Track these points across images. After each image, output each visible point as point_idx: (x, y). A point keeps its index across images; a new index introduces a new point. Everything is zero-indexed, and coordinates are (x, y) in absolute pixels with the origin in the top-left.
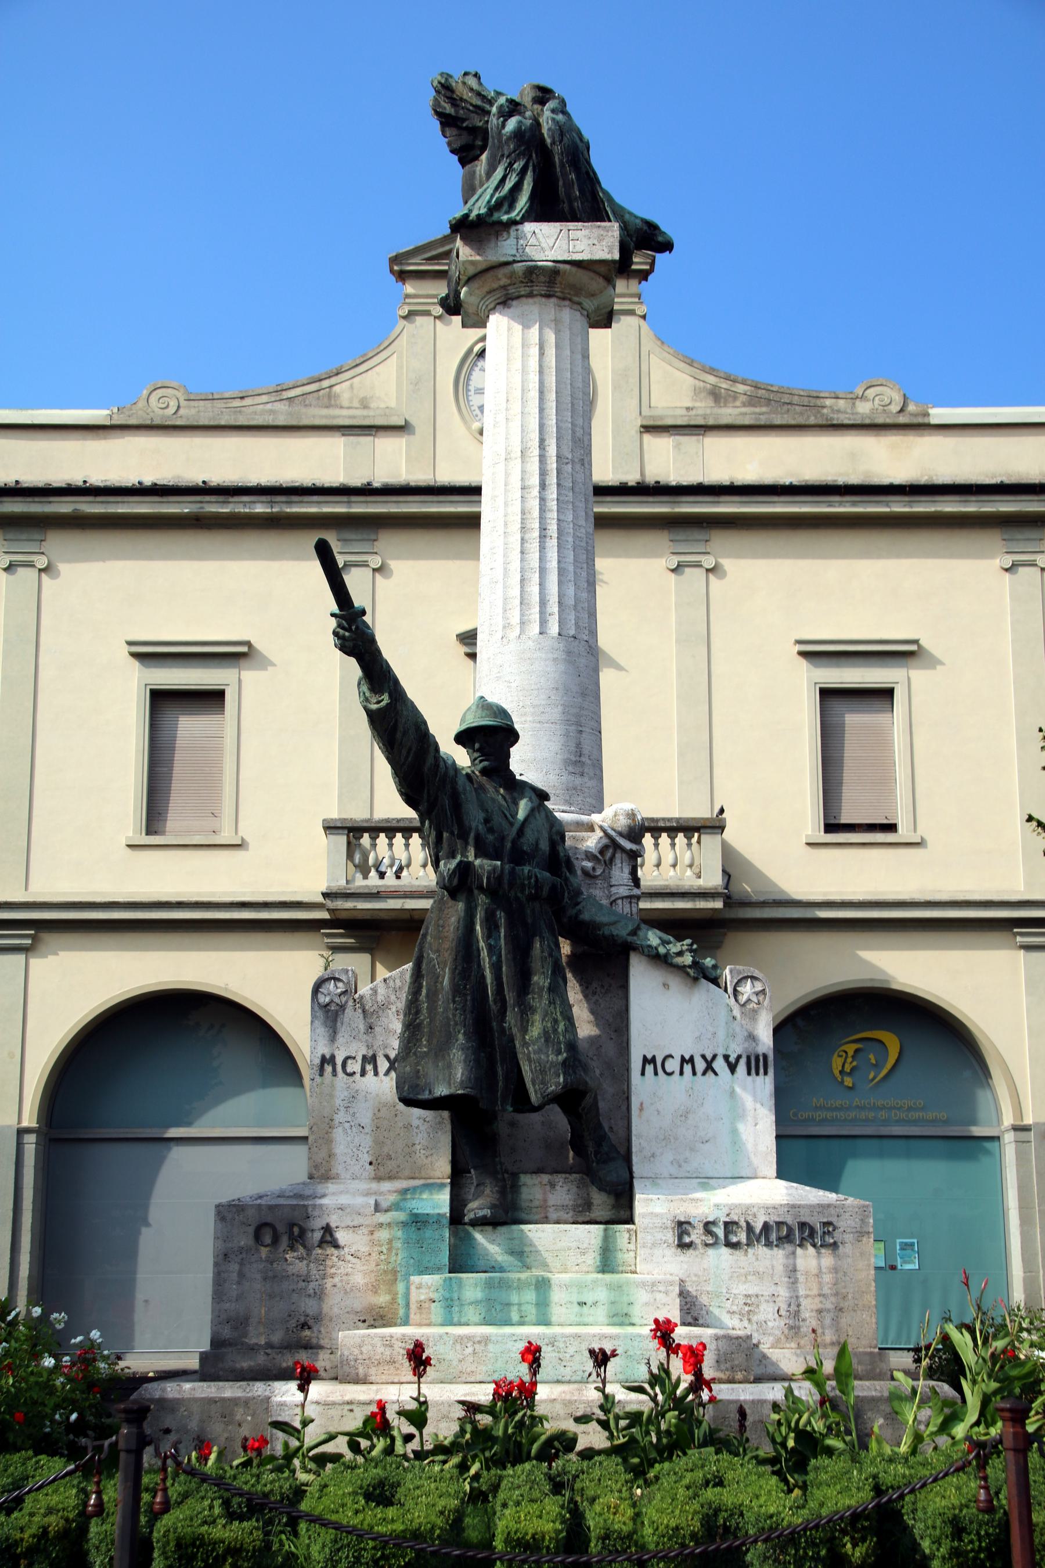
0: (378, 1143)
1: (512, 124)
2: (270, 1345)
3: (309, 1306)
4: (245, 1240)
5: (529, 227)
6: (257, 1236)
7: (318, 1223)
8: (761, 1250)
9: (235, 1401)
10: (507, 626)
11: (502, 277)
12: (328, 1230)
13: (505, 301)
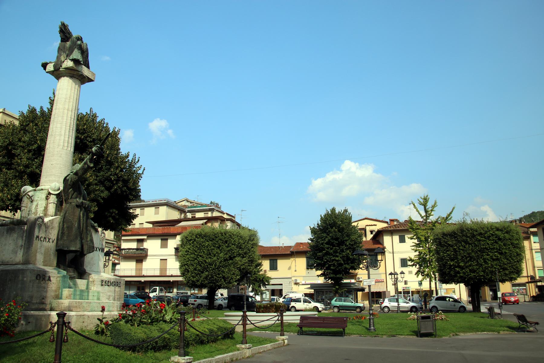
0: (45, 258)
1: (79, 42)
2: (37, 303)
3: (44, 294)
4: (34, 278)
5: (83, 66)
6: (37, 278)
7: (48, 275)
8: (111, 287)
9: (42, 315)
10: (63, 146)
11: (75, 73)
12: (49, 277)
13: (72, 76)
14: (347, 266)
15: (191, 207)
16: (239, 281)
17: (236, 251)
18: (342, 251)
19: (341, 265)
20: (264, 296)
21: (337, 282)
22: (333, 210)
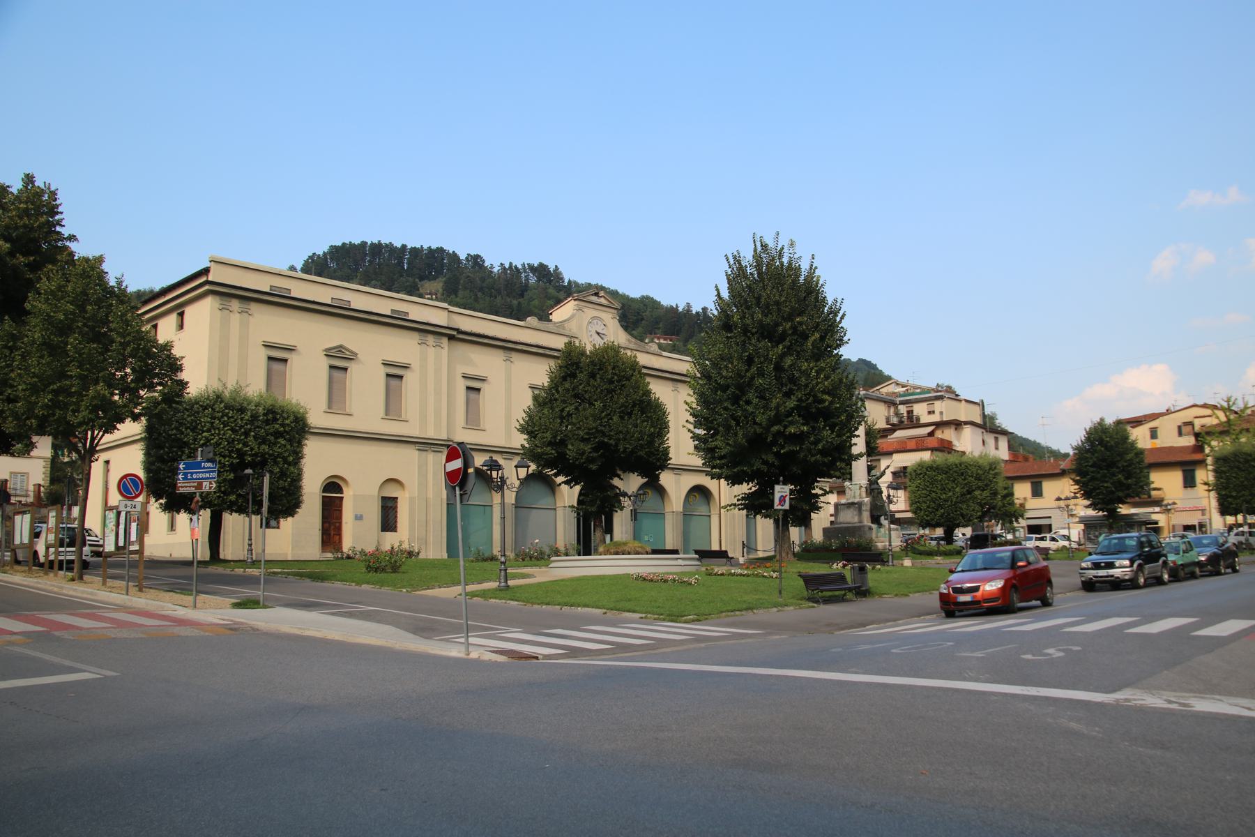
14: (1120, 494)
15: (904, 395)
16: (981, 519)
17: (975, 483)
18: (1114, 475)
19: (1113, 492)
20: (1017, 534)
21: (1113, 514)
22: (1102, 420)
